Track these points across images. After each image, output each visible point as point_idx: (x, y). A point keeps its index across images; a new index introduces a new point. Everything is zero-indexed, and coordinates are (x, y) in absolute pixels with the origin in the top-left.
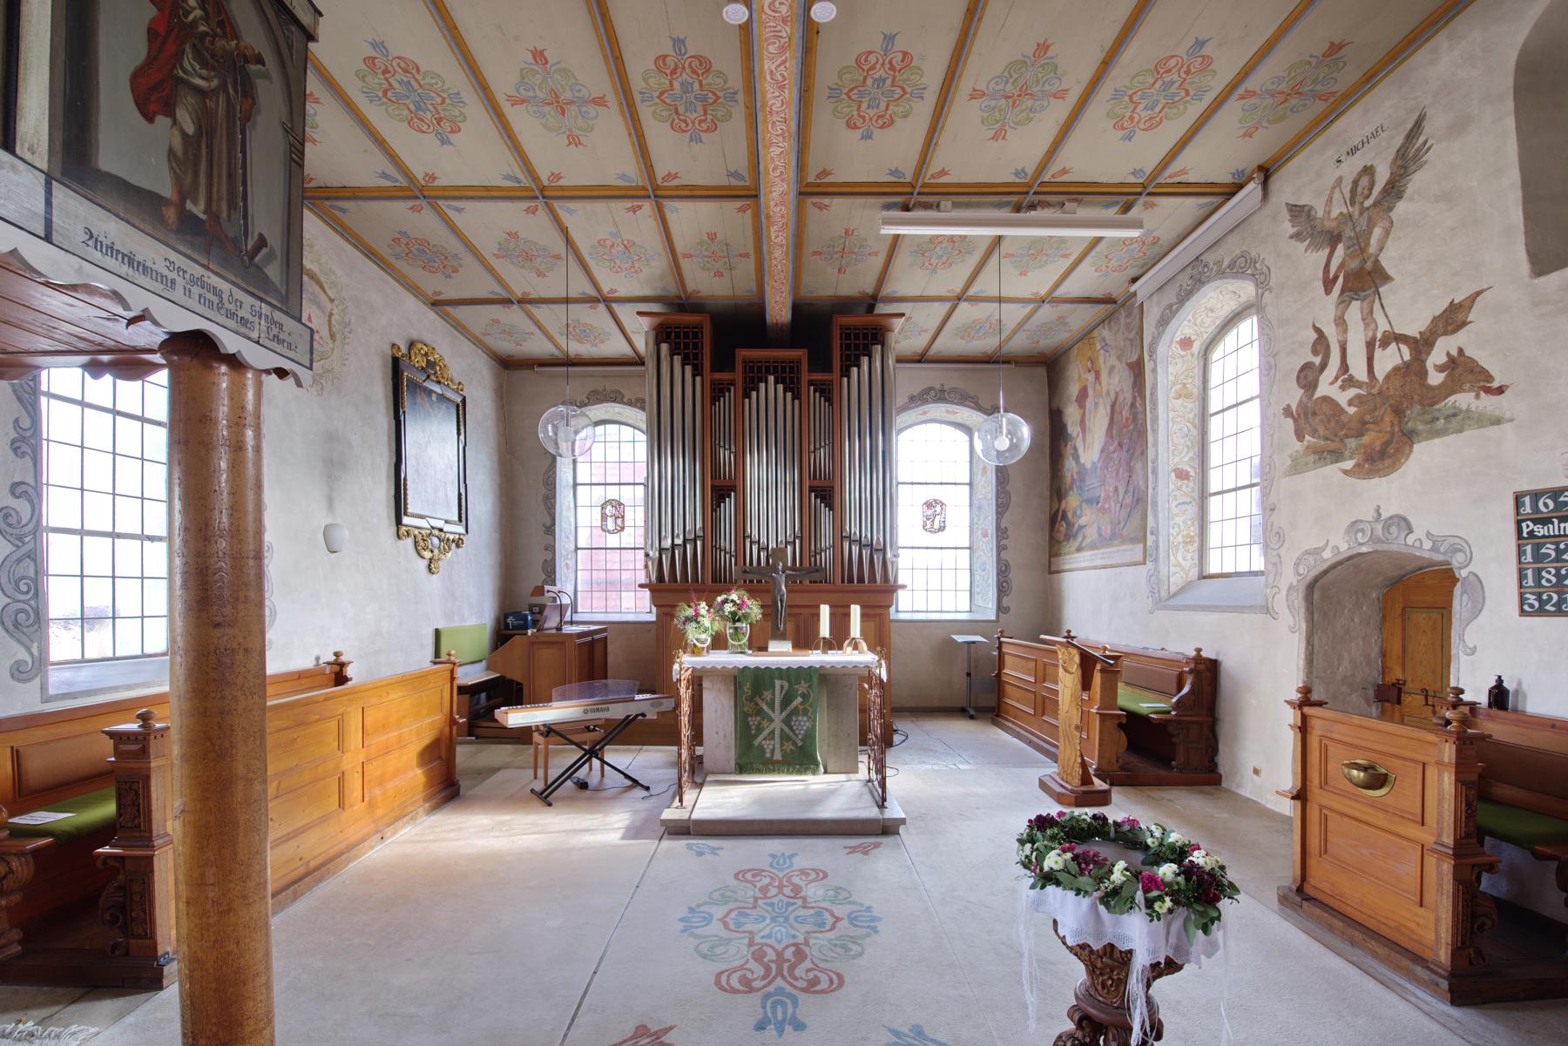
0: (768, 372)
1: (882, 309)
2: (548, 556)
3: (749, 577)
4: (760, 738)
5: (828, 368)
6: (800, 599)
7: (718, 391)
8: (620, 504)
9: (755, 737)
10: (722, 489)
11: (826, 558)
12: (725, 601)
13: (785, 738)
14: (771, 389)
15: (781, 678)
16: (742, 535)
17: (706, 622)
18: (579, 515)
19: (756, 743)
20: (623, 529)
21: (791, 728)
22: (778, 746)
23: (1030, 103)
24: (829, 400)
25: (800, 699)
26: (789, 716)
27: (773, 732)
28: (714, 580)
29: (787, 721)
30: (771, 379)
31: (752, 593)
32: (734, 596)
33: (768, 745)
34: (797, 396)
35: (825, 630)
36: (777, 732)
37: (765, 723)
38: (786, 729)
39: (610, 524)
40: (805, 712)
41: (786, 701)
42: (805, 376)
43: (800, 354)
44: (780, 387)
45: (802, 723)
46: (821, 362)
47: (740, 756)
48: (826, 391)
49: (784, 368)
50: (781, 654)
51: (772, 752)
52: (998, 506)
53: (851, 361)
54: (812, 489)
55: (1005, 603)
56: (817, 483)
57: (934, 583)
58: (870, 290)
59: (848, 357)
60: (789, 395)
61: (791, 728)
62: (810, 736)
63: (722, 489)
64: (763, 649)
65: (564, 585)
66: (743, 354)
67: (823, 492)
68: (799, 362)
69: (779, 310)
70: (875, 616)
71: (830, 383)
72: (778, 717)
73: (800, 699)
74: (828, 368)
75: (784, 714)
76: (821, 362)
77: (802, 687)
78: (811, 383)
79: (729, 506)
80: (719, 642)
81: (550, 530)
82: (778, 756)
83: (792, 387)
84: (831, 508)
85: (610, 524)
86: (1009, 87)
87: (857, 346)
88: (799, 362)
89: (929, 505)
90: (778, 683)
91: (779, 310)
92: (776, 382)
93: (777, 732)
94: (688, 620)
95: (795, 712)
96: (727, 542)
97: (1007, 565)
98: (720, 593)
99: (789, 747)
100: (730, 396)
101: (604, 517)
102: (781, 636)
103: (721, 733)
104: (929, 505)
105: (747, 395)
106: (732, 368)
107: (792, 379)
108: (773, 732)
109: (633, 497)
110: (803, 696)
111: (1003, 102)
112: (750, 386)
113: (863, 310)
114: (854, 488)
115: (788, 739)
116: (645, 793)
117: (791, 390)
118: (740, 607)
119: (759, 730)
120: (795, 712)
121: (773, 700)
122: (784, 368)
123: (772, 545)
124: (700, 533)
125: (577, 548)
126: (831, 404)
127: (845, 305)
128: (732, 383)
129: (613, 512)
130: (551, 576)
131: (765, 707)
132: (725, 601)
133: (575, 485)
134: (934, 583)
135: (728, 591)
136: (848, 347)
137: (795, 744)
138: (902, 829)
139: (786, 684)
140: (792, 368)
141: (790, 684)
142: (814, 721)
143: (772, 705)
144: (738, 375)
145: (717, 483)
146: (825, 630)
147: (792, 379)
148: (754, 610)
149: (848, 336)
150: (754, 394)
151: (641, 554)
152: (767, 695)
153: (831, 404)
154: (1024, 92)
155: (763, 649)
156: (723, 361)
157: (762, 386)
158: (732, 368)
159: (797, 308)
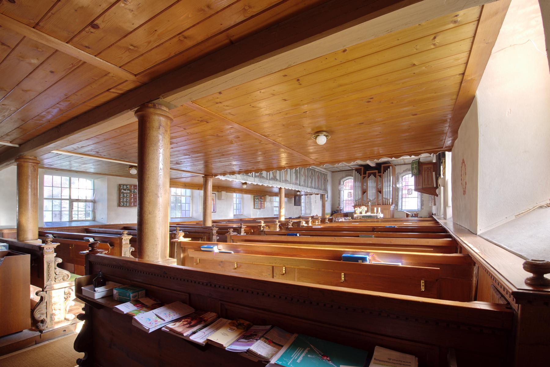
7: (364, 177)
10: (364, 192)
14: (372, 176)
42: (377, 174)
43: (377, 171)
46: (380, 172)
48: (380, 176)
53: (384, 171)
63: (364, 192)
65: (342, 206)
66: (367, 172)
76: (380, 172)
81: (339, 198)
83: (375, 176)
112: (369, 176)
130: (339, 205)
156: (365, 173)
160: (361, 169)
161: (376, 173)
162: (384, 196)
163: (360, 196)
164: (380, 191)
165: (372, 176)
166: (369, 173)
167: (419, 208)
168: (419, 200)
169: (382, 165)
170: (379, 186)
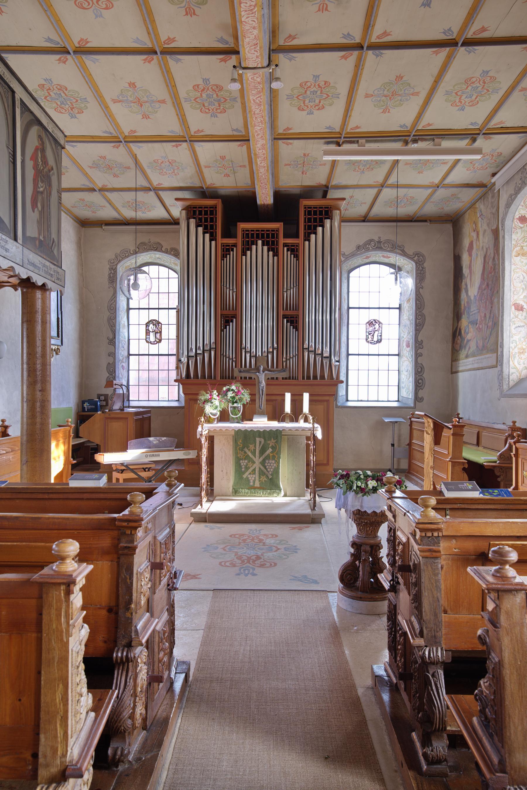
0: (258, 237)
1: (331, 194)
2: (111, 360)
3: (243, 375)
4: (247, 473)
5: (296, 236)
6: (275, 390)
8: (159, 323)
9: (244, 473)
10: (228, 317)
11: (293, 363)
12: (228, 390)
13: (261, 473)
15: (260, 437)
16: (239, 347)
17: (217, 402)
18: (133, 330)
19: (244, 476)
20: (160, 341)
21: (265, 467)
22: (257, 478)
23: (400, 98)
24: (297, 257)
25: (270, 450)
26: (264, 460)
28: (222, 377)
29: (263, 463)
30: (260, 242)
31: (245, 385)
33: (251, 478)
34: (276, 254)
35: (288, 409)
37: (250, 464)
38: (262, 467)
39: (152, 338)
40: (274, 458)
41: (263, 451)
42: (282, 240)
44: (265, 248)
47: (235, 484)
48: (294, 250)
49: (268, 235)
50: (261, 422)
52: (416, 325)
53: (311, 230)
54: (284, 317)
55: (421, 394)
56: (288, 313)
57: (373, 381)
58: (323, 182)
59: (309, 227)
60: (271, 253)
61: (265, 467)
62: (276, 471)
63: (228, 317)
66: (243, 226)
67: (291, 318)
68: (278, 230)
69: (265, 197)
71: (297, 245)
72: (258, 460)
73: (270, 450)
74: (297, 236)
75: (261, 459)
77: (272, 442)
78: (285, 245)
79: (232, 326)
80: (224, 417)
81: (112, 341)
82: (257, 484)
83: (273, 248)
84: (297, 329)
85: (152, 338)
86: (385, 92)
87: (315, 220)
88: (278, 230)
89: (371, 323)
90: (258, 440)
91: (265, 197)
92: (263, 245)
93: (257, 470)
94: (205, 402)
95: (268, 458)
96: (230, 353)
97: (422, 368)
98: (225, 385)
99: (264, 479)
100: (233, 254)
101: (148, 332)
102: (261, 414)
103: (225, 471)
105: (244, 254)
106: (233, 236)
107: (273, 242)
108: (254, 470)
109: (169, 319)
110: (273, 447)
111: (384, 98)
112: (246, 248)
113: (320, 194)
114: (311, 317)
117: (273, 250)
118: (238, 393)
119: (247, 468)
120: (268, 458)
121: (255, 450)
122: (268, 235)
123: (259, 354)
124: (213, 346)
125: (129, 355)
126: (298, 259)
127: (308, 192)
128: (235, 245)
129: (154, 327)
131: (250, 454)
132: (228, 390)
133: (129, 309)
134: (373, 381)
135: (230, 384)
136: (309, 220)
137: (267, 477)
139: (263, 440)
140: (273, 235)
141: (265, 440)
142: (279, 463)
143: (254, 453)
144: (239, 240)
145: (225, 312)
146: (288, 409)
147: (273, 242)
149: (309, 213)
150: (249, 253)
151: (173, 359)
152: (252, 447)
153: (298, 259)
154: (394, 94)
156: (228, 233)
157: (254, 247)
158: (235, 237)
159: (277, 195)
160: (212, 210)
161: (274, 234)
162: (309, 342)
163: (210, 338)
165: (259, 249)
166: (247, 234)
167: (408, 392)
168: (408, 365)
169: (305, 202)
170: (290, 294)
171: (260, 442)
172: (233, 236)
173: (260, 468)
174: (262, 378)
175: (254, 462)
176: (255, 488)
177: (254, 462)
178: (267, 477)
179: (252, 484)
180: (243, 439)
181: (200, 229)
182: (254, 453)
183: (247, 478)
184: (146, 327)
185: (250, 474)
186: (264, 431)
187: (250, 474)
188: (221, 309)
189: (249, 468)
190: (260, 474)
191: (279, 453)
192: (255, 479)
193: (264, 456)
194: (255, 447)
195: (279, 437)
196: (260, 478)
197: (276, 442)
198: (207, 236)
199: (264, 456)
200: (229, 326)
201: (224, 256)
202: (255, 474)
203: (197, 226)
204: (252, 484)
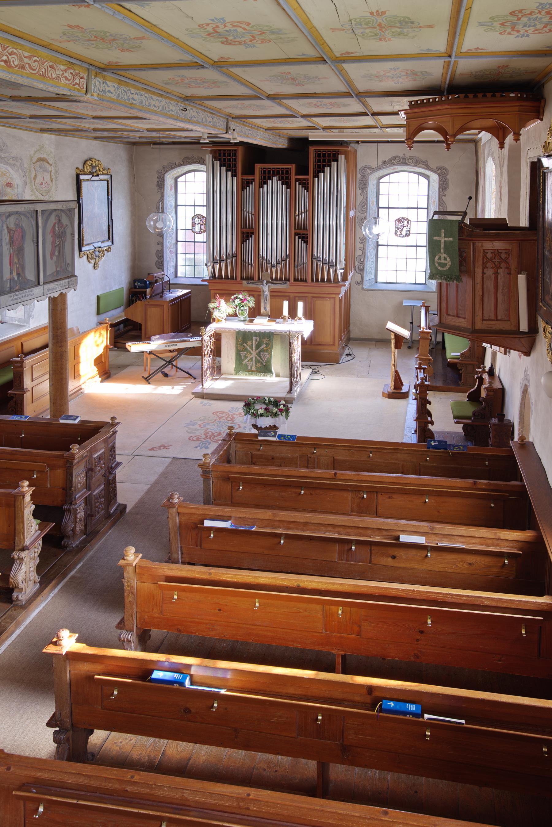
13: (257, 361)
15: (256, 336)
21: (260, 357)
22: (254, 364)
26: (260, 352)
27: (252, 359)
29: (259, 354)
32: (240, 296)
33: (249, 364)
36: (254, 359)
37: (248, 355)
38: (258, 357)
40: (267, 351)
41: (258, 346)
45: (265, 355)
51: (251, 367)
61: (260, 357)
64: (251, 321)
70: (333, 298)
72: (254, 352)
73: (264, 345)
75: (257, 351)
77: (266, 340)
79: (251, 240)
82: (254, 369)
93: (254, 359)
95: (262, 350)
99: (259, 365)
104: (399, 221)
108: (252, 359)
110: (266, 344)
115: (259, 362)
116: (193, 381)
120: (262, 350)
121: (252, 345)
131: (248, 348)
137: (262, 364)
138: (294, 402)
139: (258, 339)
141: (260, 338)
142: (271, 355)
143: (252, 348)
145: (245, 231)
148: (252, 304)
155: (251, 321)
164: (302, 233)
171: (256, 340)
172: (251, 172)
173: (256, 358)
174: (266, 289)
175: (251, 354)
176: (252, 371)
177: (251, 354)
178: (262, 364)
179: (249, 368)
180: (243, 337)
181: (224, 168)
182: (252, 348)
183: (246, 365)
184: (193, 220)
185: (248, 361)
186: (260, 332)
187: (248, 361)
188: (241, 228)
189: (247, 357)
190: (256, 362)
191: (271, 349)
192: (252, 365)
193: (259, 350)
194: (252, 343)
195: (272, 337)
196: (256, 364)
197: (269, 340)
198: (230, 173)
199: (259, 350)
200: (249, 240)
201: (244, 188)
202: (252, 361)
203: (221, 166)
204: (249, 368)
